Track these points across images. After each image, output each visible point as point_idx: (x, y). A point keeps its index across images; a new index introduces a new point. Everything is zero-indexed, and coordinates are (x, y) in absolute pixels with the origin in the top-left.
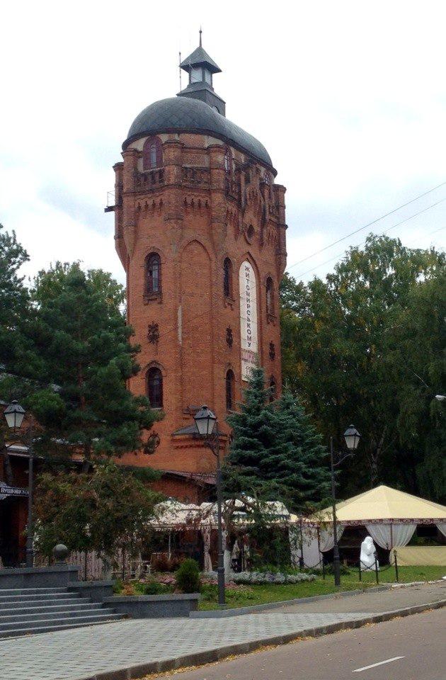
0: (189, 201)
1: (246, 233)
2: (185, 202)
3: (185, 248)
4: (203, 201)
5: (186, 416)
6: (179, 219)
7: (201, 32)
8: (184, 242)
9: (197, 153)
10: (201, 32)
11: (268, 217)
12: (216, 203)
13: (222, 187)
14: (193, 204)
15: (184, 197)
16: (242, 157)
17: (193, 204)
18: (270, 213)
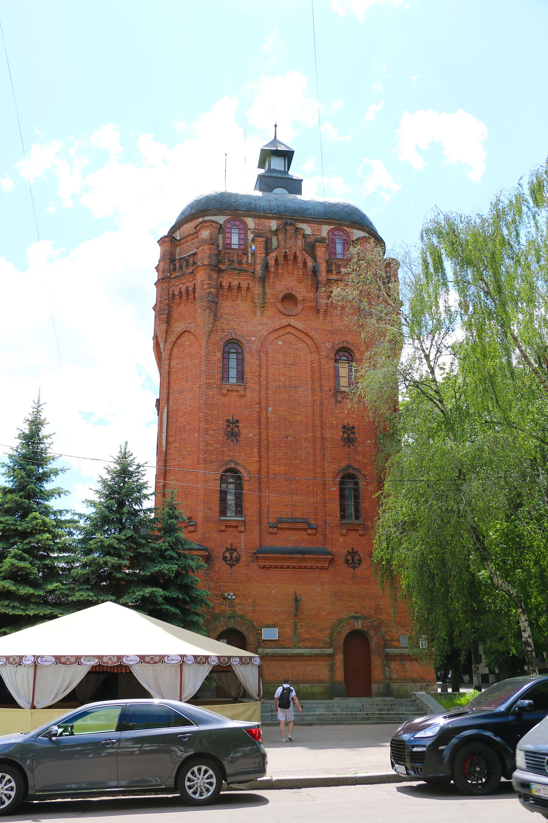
0: (176, 293)
1: (279, 305)
2: (173, 294)
3: (174, 343)
4: (190, 285)
5: (271, 530)
6: (162, 314)
7: (276, 126)
8: (173, 338)
9: (193, 239)
10: (276, 126)
11: (323, 276)
12: (199, 282)
13: (206, 263)
14: (180, 292)
15: (171, 290)
16: (274, 224)
17: (180, 292)
18: (329, 271)
